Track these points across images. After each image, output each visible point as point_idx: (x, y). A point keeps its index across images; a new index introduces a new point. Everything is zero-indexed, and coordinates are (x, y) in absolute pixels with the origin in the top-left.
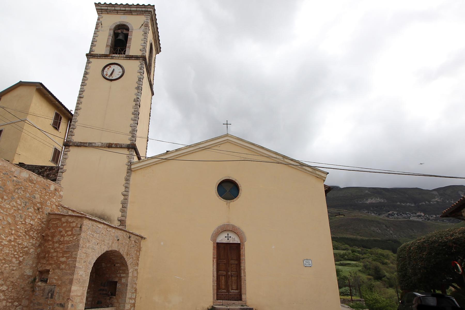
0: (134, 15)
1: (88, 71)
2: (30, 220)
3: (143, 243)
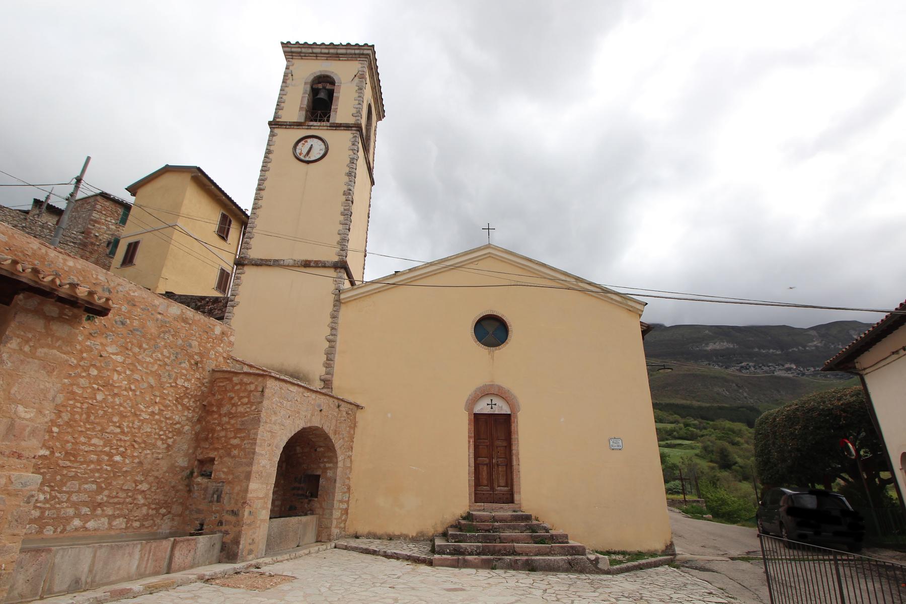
1: (272, 148)
2: (183, 381)
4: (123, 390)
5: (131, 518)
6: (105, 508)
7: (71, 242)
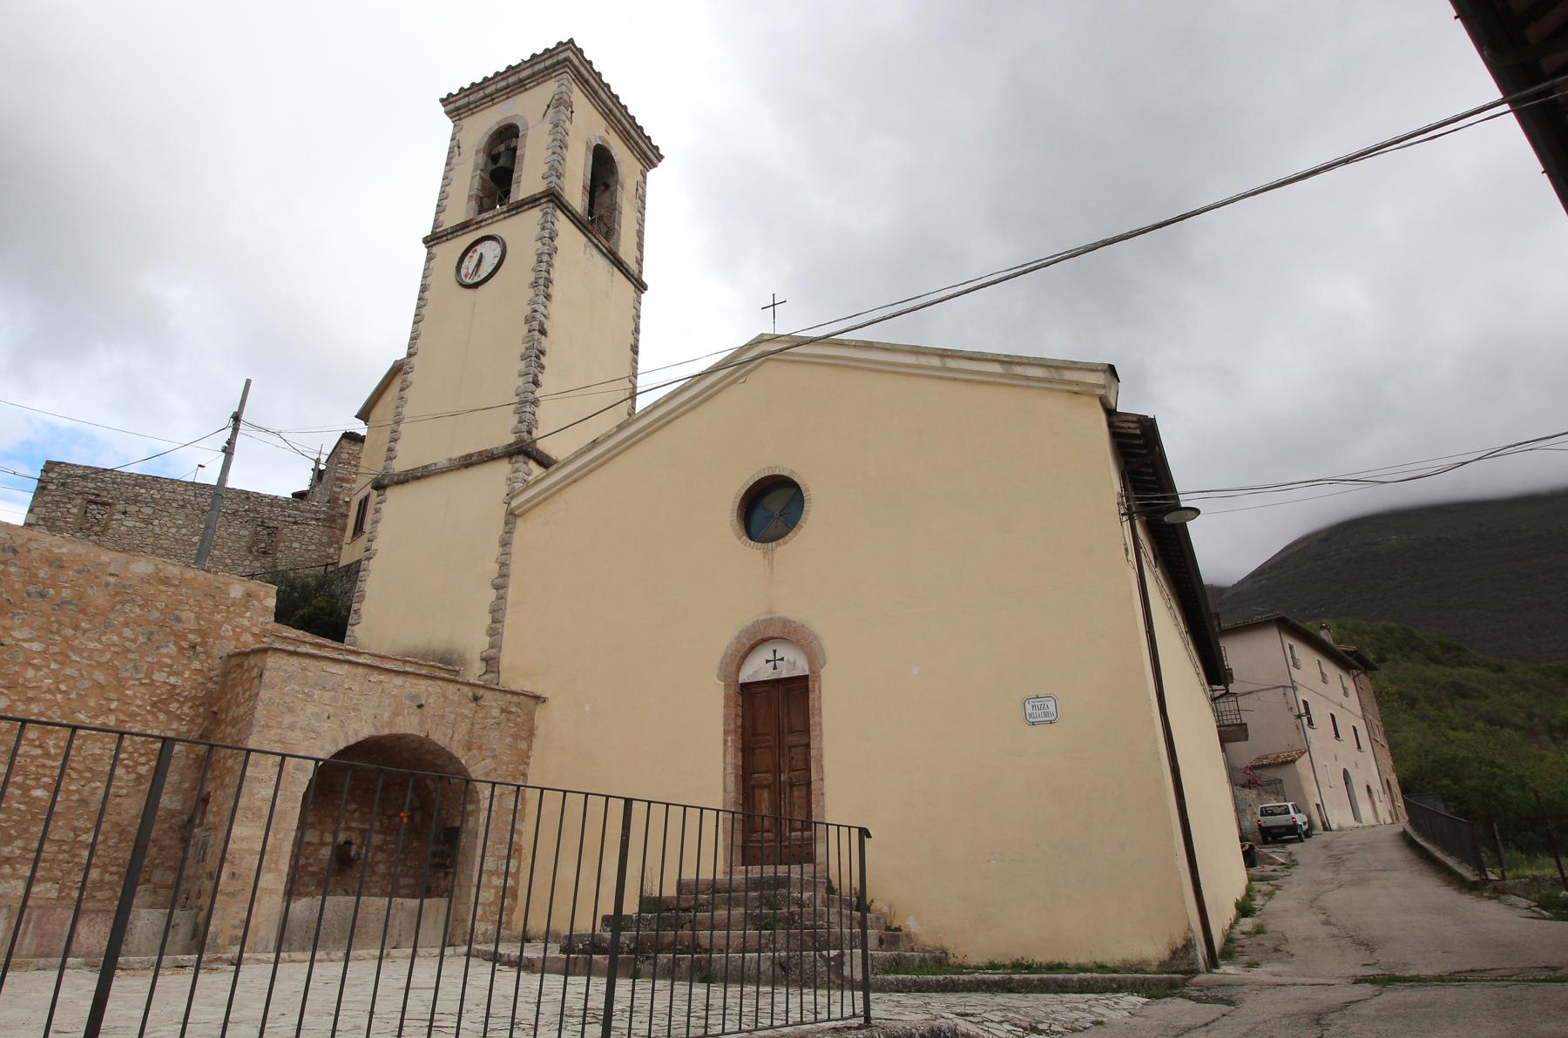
0: (530, 88)
1: (428, 281)
2: (165, 675)
3: (540, 714)
4: (45, 692)
5: (68, 884)
6: (18, 866)
7: (312, 519)
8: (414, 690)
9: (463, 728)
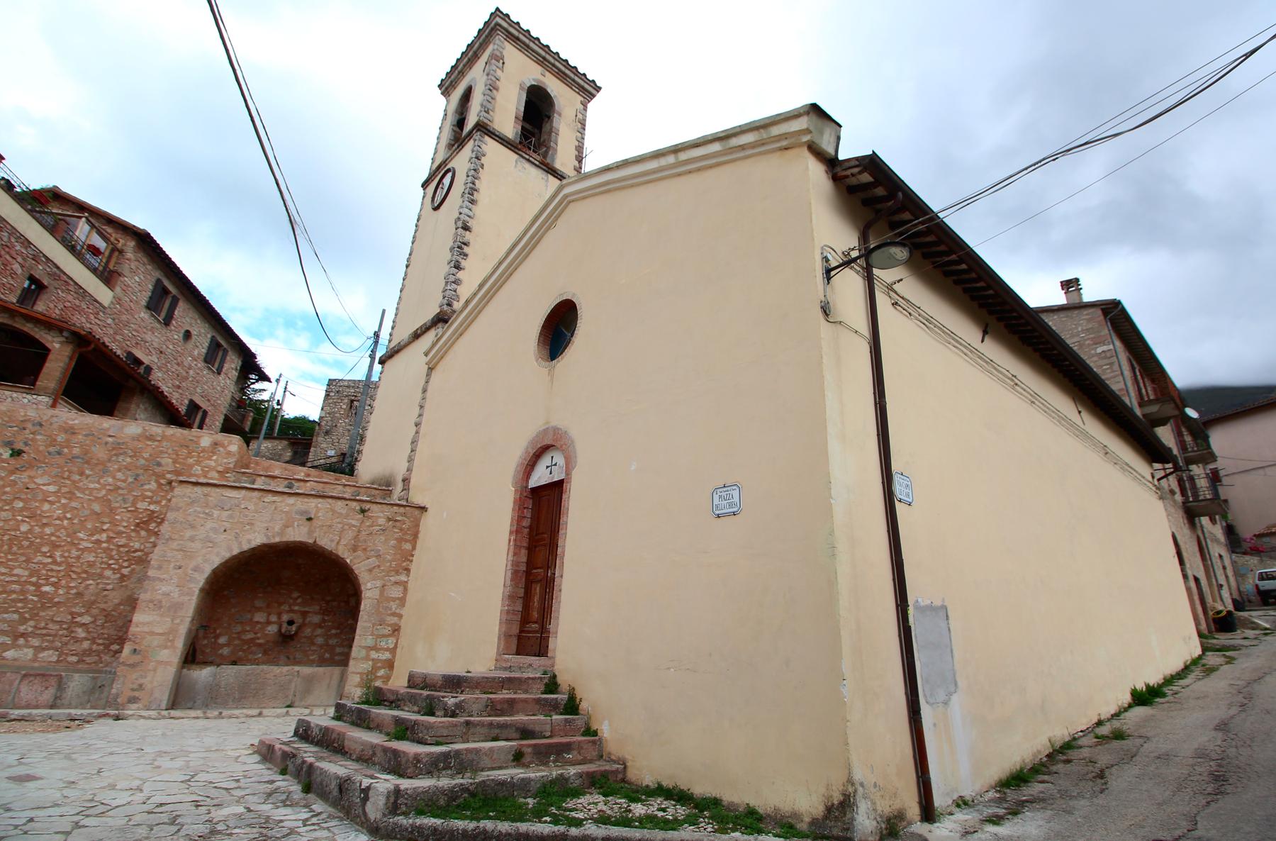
4: (56, 519)
6: (30, 639)
8: (303, 507)
9: (350, 534)
